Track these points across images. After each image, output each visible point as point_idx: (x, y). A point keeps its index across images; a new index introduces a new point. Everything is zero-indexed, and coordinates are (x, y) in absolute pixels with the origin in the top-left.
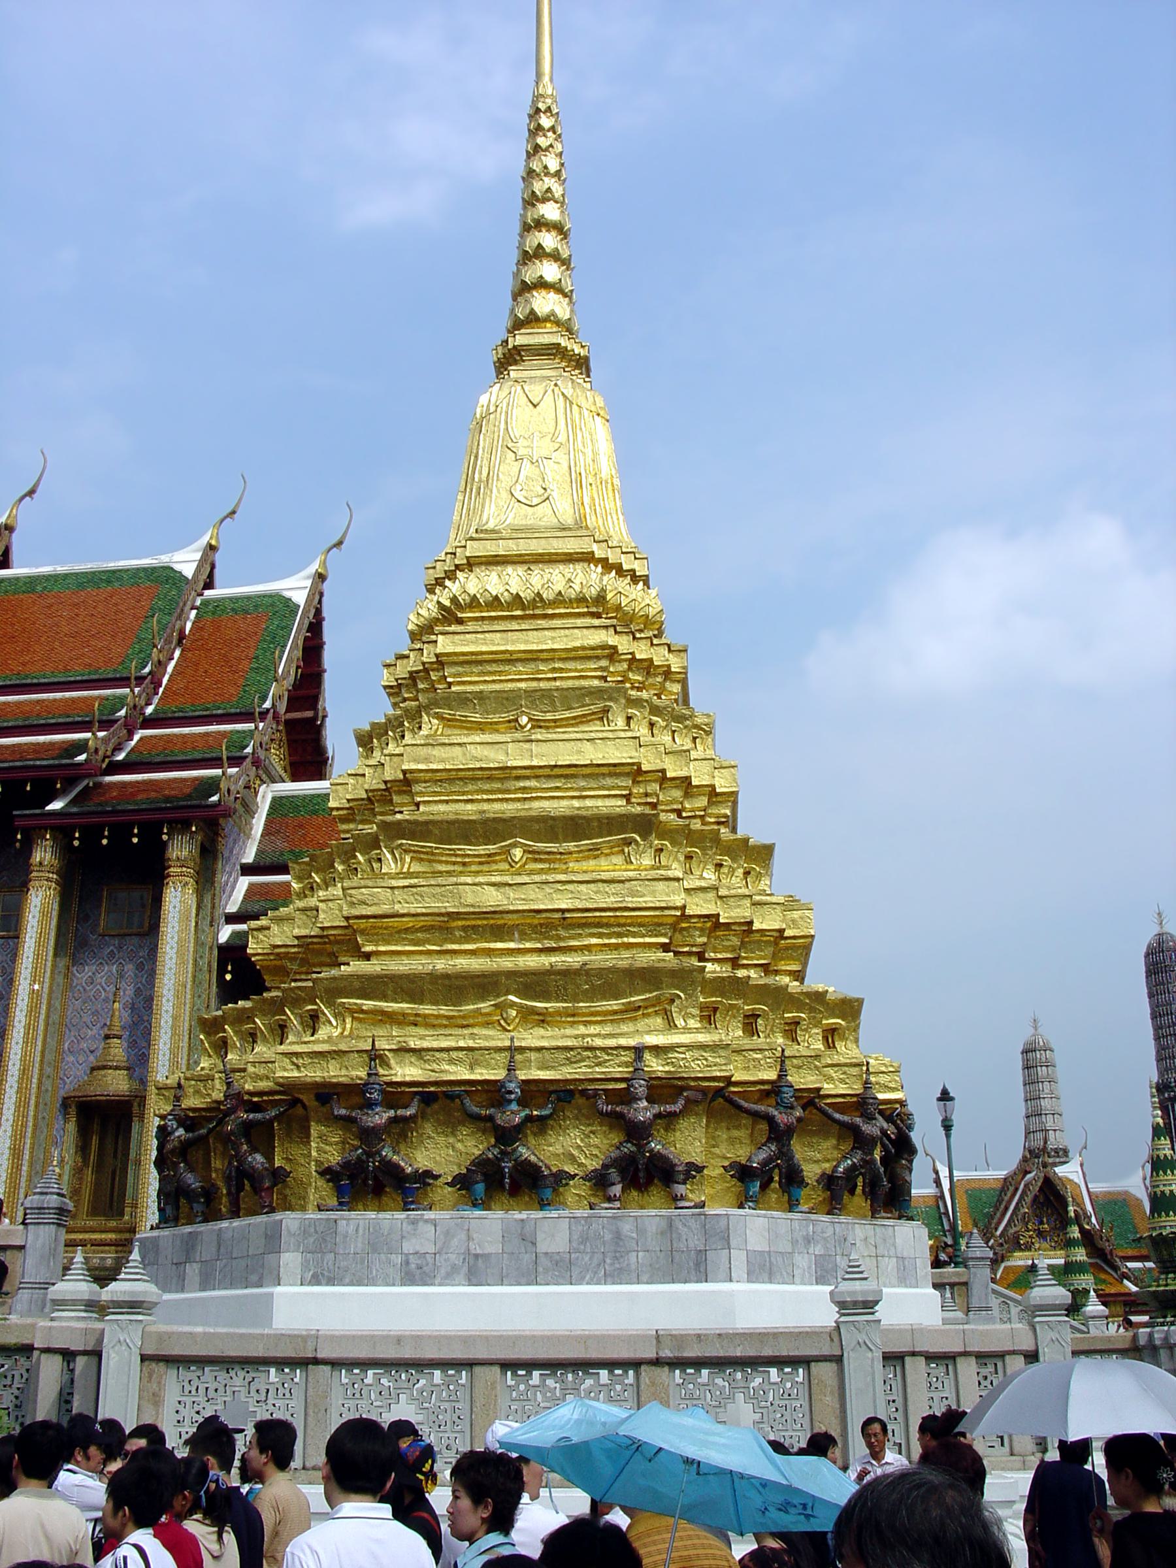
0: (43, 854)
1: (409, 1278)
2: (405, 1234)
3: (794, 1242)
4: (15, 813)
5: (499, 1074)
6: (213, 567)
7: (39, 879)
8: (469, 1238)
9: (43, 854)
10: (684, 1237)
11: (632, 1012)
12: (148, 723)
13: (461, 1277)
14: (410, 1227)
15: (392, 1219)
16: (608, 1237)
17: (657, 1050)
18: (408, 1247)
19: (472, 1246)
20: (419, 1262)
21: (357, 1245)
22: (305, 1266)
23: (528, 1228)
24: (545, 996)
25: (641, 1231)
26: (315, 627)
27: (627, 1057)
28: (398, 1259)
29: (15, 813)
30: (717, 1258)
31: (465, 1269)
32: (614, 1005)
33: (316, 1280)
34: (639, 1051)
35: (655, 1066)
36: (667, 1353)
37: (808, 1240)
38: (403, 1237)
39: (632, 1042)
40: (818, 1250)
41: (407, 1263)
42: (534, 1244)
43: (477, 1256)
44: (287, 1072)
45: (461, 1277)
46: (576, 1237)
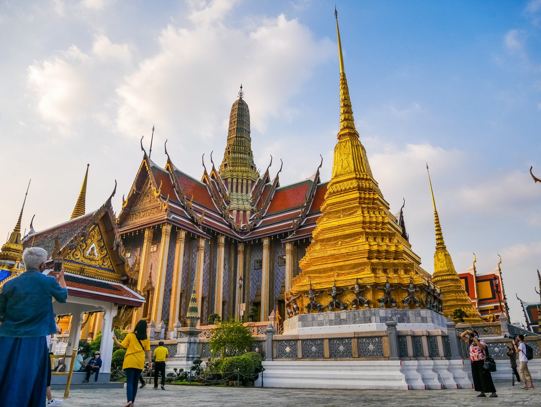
0: (288, 247)
1: (319, 325)
3: (392, 315)
5: (331, 286)
6: (319, 178)
9: (288, 247)
11: (358, 272)
12: (307, 216)
15: (315, 314)
17: (361, 279)
18: (319, 319)
24: (342, 270)
27: (355, 280)
30: (373, 318)
32: (355, 270)
34: (357, 279)
35: (360, 281)
36: (356, 336)
37: (396, 314)
39: (356, 277)
40: (399, 316)
44: (298, 289)
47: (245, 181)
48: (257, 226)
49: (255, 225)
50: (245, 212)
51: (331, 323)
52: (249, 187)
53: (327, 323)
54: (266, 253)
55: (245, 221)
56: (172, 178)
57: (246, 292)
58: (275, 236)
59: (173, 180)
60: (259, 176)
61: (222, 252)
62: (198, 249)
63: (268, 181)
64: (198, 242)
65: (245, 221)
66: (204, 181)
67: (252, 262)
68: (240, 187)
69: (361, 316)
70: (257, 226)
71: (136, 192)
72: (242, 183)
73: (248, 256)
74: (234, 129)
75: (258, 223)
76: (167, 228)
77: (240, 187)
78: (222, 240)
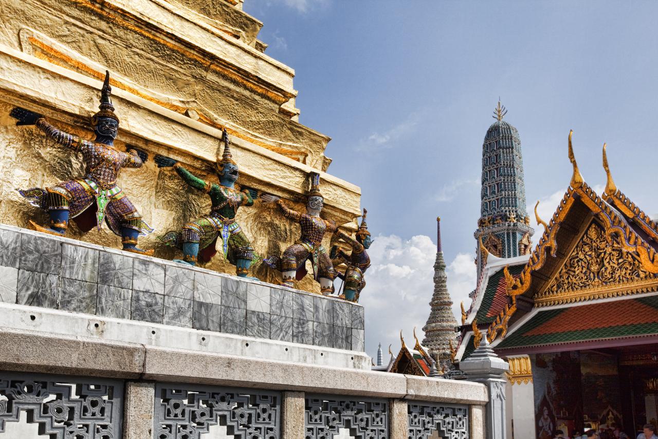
2: (136, 272)
8: (194, 288)
10: (340, 317)
13: (186, 320)
14: (141, 267)
16: (295, 307)
18: (139, 284)
19: (196, 295)
20: (149, 300)
21: (86, 273)
22: (22, 285)
23: (242, 289)
25: (316, 308)
28: (129, 294)
31: (189, 314)
33: (36, 299)
38: (134, 275)
41: (138, 300)
42: (245, 302)
43: (201, 304)
45: (186, 320)
46: (274, 303)
51: (199, 316)
53: (180, 313)
69: (323, 317)
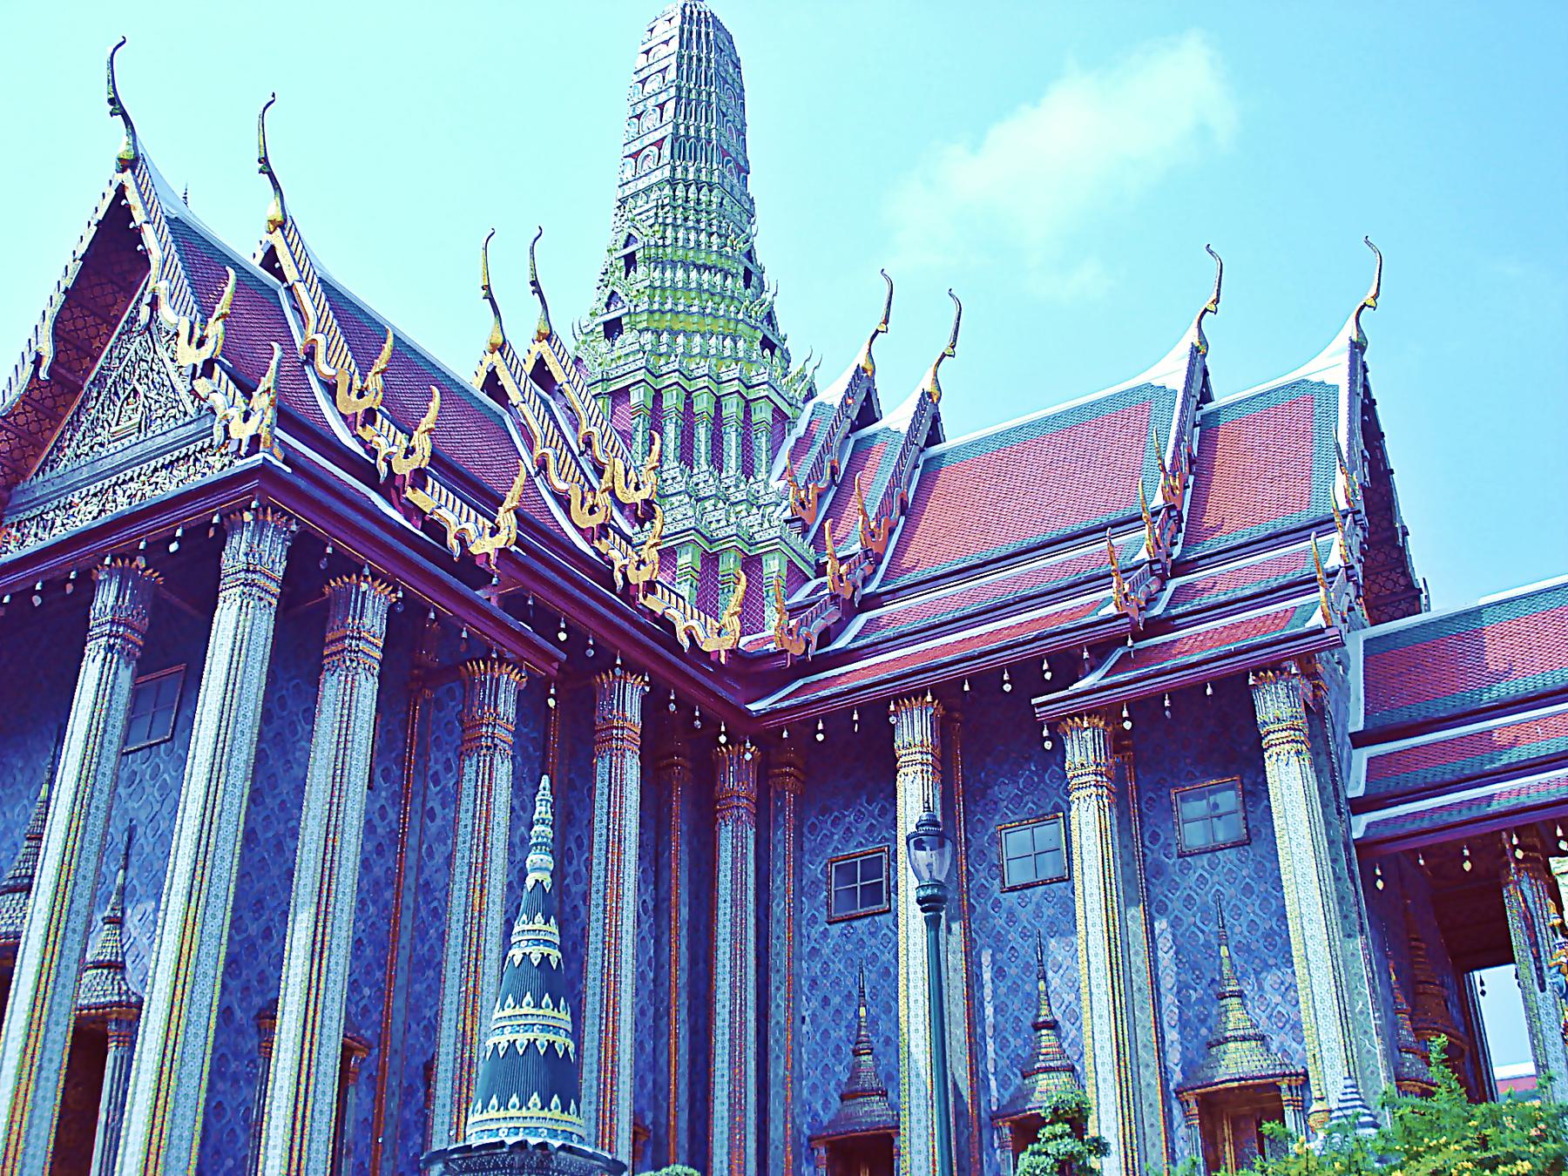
0: (1082, 751)
4: (1034, 701)
7: (1084, 786)
9: (1082, 751)
26: (1367, 408)
29: (1034, 701)
47: (732, 408)
48: (840, 644)
49: (826, 637)
50: (751, 564)
52: (762, 443)
54: (914, 796)
55: (750, 616)
56: (297, 309)
57: (777, 1071)
58: (986, 680)
59: (304, 324)
60: (811, 395)
61: (622, 780)
62: (468, 741)
63: (868, 414)
64: (469, 687)
65: (750, 616)
66: (492, 384)
67: (815, 870)
68: (702, 434)
70: (840, 644)
71: (51, 372)
72: (718, 421)
73: (783, 838)
74: (659, 144)
75: (841, 626)
76: (253, 554)
77: (702, 434)
78: (628, 703)
